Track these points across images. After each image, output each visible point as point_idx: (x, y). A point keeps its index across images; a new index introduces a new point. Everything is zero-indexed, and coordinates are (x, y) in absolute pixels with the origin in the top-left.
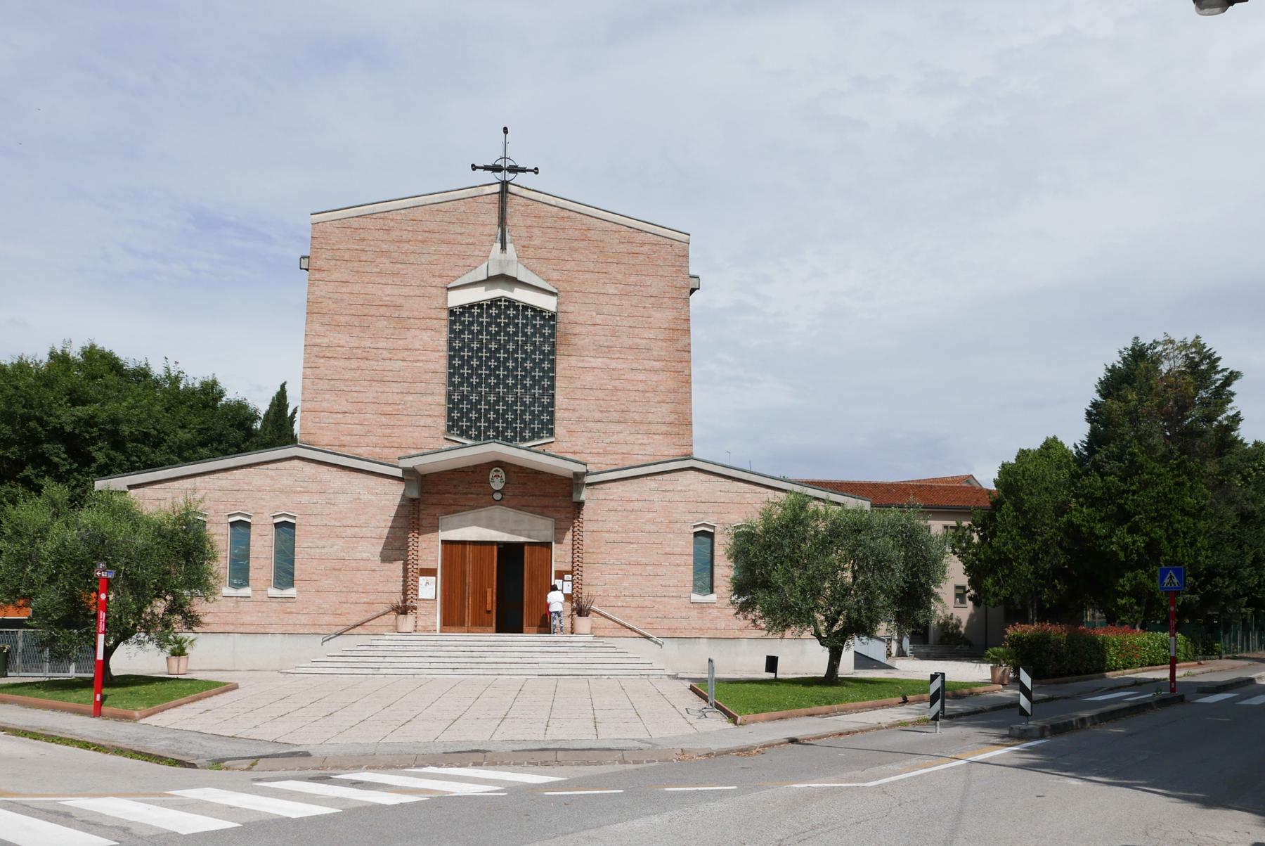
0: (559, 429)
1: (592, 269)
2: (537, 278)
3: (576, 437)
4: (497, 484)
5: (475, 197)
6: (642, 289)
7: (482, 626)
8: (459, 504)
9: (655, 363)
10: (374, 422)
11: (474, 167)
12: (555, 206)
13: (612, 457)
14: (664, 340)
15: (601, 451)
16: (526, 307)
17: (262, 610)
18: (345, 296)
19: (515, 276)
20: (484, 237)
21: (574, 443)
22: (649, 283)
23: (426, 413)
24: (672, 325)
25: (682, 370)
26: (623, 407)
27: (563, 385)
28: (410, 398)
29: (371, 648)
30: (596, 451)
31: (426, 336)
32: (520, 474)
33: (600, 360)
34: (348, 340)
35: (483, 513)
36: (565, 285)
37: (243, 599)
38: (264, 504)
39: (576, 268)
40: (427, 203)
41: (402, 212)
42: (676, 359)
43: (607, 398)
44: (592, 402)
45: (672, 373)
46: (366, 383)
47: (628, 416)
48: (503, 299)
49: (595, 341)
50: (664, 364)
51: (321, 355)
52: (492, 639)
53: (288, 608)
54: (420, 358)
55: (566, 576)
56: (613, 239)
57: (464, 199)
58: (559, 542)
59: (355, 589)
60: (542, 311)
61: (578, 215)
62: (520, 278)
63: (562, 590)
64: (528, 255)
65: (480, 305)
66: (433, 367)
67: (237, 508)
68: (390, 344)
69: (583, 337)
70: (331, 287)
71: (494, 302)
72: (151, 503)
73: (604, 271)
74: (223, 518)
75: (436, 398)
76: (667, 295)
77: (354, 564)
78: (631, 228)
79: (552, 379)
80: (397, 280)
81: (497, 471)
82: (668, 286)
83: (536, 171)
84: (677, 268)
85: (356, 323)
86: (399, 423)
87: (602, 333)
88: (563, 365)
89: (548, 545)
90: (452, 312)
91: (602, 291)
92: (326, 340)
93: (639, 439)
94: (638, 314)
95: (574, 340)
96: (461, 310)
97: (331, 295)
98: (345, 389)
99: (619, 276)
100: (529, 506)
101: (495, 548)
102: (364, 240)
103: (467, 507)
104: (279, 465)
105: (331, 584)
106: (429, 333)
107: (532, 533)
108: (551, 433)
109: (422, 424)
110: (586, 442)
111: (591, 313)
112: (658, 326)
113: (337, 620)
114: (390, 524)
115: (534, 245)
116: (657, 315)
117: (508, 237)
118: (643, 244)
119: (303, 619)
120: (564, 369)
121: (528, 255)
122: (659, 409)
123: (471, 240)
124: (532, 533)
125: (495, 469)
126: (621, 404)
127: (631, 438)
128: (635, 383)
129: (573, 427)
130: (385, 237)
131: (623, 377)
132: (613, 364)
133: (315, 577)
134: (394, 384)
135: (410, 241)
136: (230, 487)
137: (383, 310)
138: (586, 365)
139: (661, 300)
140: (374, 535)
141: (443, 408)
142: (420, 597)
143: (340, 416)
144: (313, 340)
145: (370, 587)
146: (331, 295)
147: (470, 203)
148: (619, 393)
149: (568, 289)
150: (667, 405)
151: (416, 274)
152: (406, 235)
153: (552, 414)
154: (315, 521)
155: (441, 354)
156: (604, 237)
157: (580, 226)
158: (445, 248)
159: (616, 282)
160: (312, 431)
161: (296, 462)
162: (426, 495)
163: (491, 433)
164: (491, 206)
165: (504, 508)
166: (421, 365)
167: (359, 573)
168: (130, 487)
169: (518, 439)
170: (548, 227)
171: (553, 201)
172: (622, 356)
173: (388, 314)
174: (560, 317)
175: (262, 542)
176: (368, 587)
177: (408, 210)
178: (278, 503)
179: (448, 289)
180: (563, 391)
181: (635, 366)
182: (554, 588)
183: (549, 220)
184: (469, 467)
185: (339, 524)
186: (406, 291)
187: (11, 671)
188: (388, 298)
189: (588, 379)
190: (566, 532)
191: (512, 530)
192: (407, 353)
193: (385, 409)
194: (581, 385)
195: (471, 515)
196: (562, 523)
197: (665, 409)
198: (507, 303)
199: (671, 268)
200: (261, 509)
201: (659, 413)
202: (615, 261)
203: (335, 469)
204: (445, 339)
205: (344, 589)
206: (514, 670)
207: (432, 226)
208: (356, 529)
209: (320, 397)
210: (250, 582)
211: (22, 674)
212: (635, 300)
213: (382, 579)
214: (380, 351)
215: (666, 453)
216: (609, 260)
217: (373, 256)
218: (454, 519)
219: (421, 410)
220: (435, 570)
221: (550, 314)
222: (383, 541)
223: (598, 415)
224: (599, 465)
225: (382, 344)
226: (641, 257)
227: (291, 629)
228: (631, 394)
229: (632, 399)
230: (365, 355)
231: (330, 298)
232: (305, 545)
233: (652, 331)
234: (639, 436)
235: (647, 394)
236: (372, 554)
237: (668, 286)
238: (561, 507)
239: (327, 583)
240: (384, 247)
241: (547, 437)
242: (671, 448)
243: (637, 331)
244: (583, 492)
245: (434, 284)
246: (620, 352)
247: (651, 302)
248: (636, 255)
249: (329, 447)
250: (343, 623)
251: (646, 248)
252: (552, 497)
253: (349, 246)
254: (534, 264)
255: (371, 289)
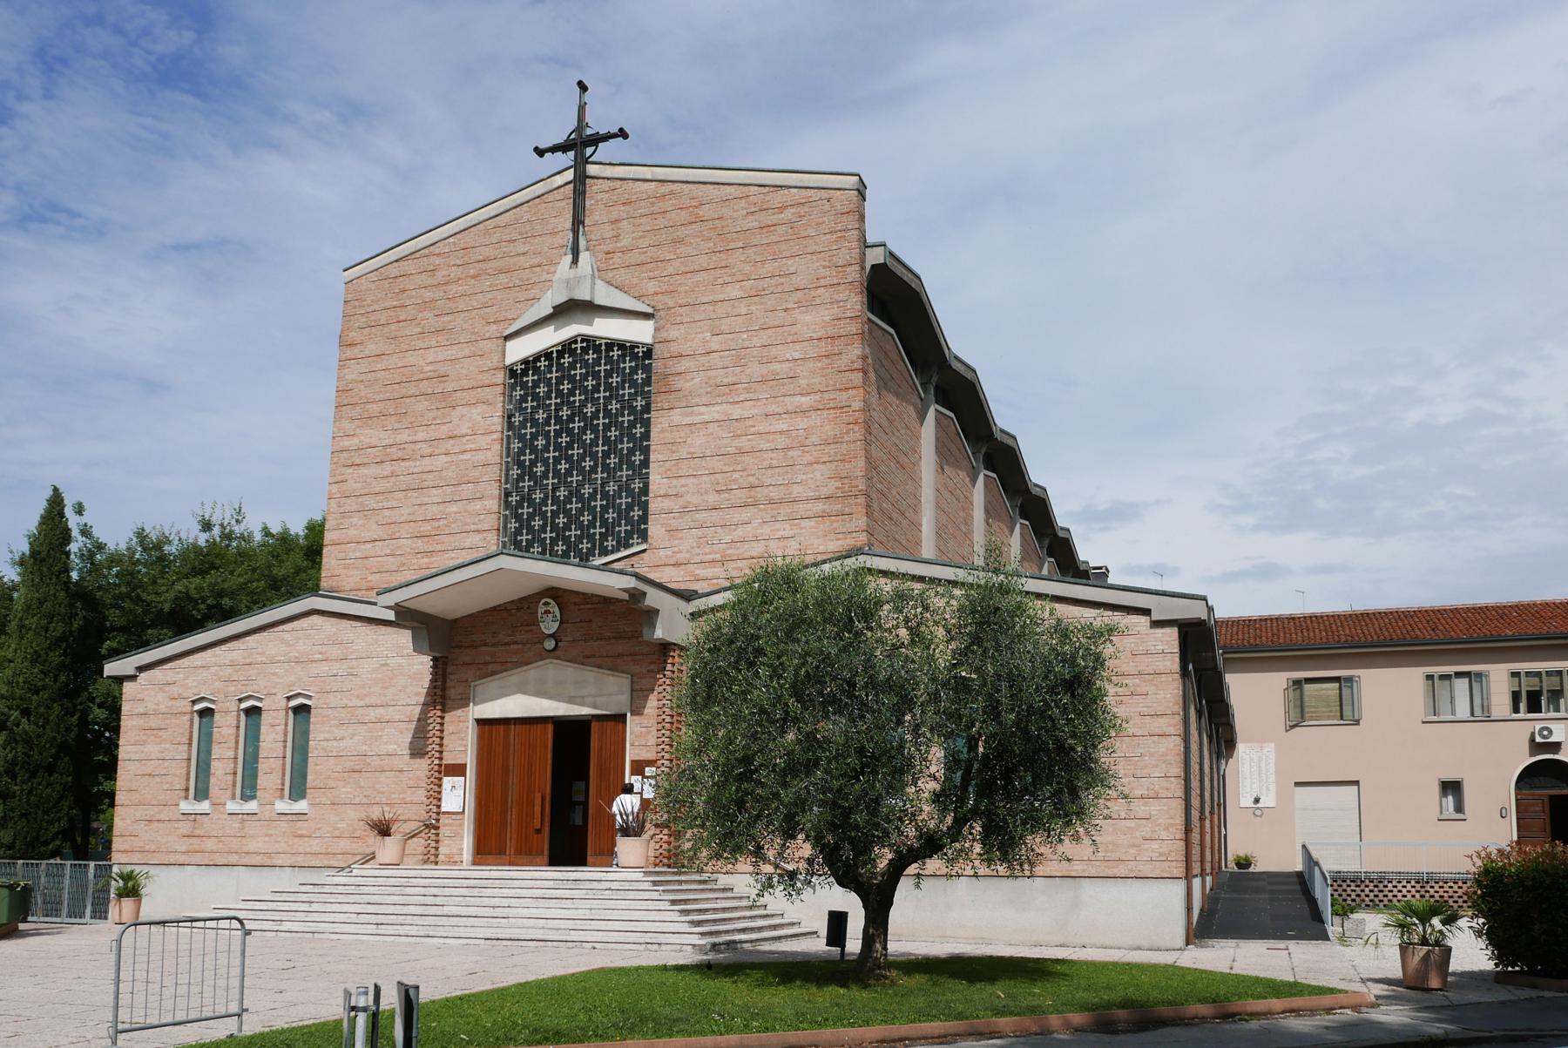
0: (655, 529)
1: (705, 265)
2: (625, 296)
3: (681, 539)
4: (550, 626)
5: (543, 195)
6: (782, 280)
7: (530, 855)
8: (498, 660)
9: (803, 399)
10: (408, 550)
11: (540, 152)
12: (652, 181)
13: (735, 566)
14: (819, 358)
15: (718, 557)
16: (611, 345)
17: (270, 832)
18: (379, 375)
19: (588, 298)
20: (554, 251)
21: (675, 549)
22: (792, 269)
23: (473, 527)
24: (831, 331)
25: (847, 404)
26: (751, 479)
27: (661, 457)
28: (454, 508)
29: (316, 889)
30: (710, 557)
31: (475, 413)
32: (582, 607)
33: (717, 408)
34: (381, 436)
35: (531, 673)
36: (665, 298)
37: (249, 818)
38: (278, 680)
39: (683, 269)
40: (481, 219)
41: (451, 240)
42: (838, 386)
43: (726, 469)
44: (704, 478)
45: (832, 411)
46: (401, 495)
47: (760, 493)
48: (579, 339)
49: (709, 378)
50: (817, 397)
51: (349, 462)
52: (544, 875)
53: (300, 829)
54: (468, 447)
55: (647, 769)
56: (737, 211)
57: (527, 202)
58: (638, 711)
59: (378, 800)
60: (634, 346)
61: (685, 186)
62: (599, 301)
63: (641, 794)
64: (614, 264)
65: (547, 355)
66: (483, 458)
67: (248, 688)
68: (432, 433)
69: (691, 375)
70: (364, 366)
71: (567, 347)
72: (160, 689)
73: (723, 264)
74: (233, 703)
75: (486, 503)
76: (823, 282)
77: (376, 762)
78: (764, 186)
79: (646, 451)
80: (441, 339)
81: (546, 604)
82: (824, 267)
83: (622, 134)
84: (839, 234)
85: (392, 411)
86: (439, 547)
87: (720, 364)
88: (663, 425)
89: (620, 718)
90: (512, 373)
91: (721, 297)
92: (355, 441)
93: (778, 530)
94: (776, 323)
95: (679, 383)
96: (523, 366)
97: (363, 377)
98: (375, 506)
99: (747, 268)
100: (594, 656)
101: (550, 727)
102: (403, 291)
103: (509, 665)
104: (296, 624)
105: (350, 793)
106: (481, 408)
107: (599, 700)
108: (644, 536)
109: (468, 545)
110: (695, 545)
111: (703, 336)
112: (807, 336)
113: (354, 845)
114: (422, 700)
115: (623, 247)
116: (807, 318)
117: (582, 243)
118: (782, 209)
119: (315, 845)
120: (663, 431)
121: (614, 264)
122: (812, 476)
123: (536, 261)
124: (599, 700)
125: (543, 601)
126: (748, 475)
127: (765, 531)
128: (771, 437)
129: (675, 524)
130: (430, 281)
131: (753, 430)
132: (737, 412)
133: (331, 783)
134: (434, 491)
135: (459, 279)
136: (242, 661)
137: (424, 386)
138: (696, 419)
139: (813, 293)
140: (403, 718)
141: (495, 516)
142: (443, 810)
143: (369, 546)
144: (341, 444)
145: (396, 796)
146: (363, 377)
147: (536, 205)
148: (746, 458)
149: (671, 304)
150: (822, 466)
151: (465, 326)
152: (456, 272)
153: (644, 507)
154: (334, 700)
155: (495, 436)
156: (724, 210)
157: (687, 203)
158: (503, 279)
159: (741, 278)
160: (337, 572)
161: (315, 619)
162: (457, 650)
163: (537, 549)
164: (563, 204)
165: (559, 661)
166: (469, 457)
167: (383, 775)
168: (141, 669)
169: (597, 552)
170: (642, 216)
171: (646, 173)
172: (752, 396)
173: (430, 391)
174: (657, 353)
175: (274, 736)
176: (393, 796)
177: (458, 236)
178: (292, 678)
179: (507, 338)
180: (661, 466)
181: (772, 408)
182: (629, 789)
183: (643, 203)
184: (513, 601)
185: (361, 703)
186: (451, 352)
187: (33, 915)
188: (430, 368)
189: (698, 442)
190: (648, 696)
191: (571, 697)
192: (452, 442)
193: (422, 529)
194: (688, 453)
195: (515, 677)
196: (643, 681)
197: (820, 472)
198: (585, 344)
199: (828, 236)
200: (274, 688)
201: (810, 481)
202: (741, 245)
203: (359, 624)
204: (501, 414)
205: (365, 800)
206: (461, 929)
207: (487, 252)
208: (381, 710)
209: (346, 523)
210: (258, 793)
211: (42, 919)
212: (770, 302)
213: (411, 783)
214: (419, 445)
215: (822, 549)
216: (732, 245)
217: (413, 312)
218: (492, 684)
219: (466, 524)
220: (464, 766)
221: (645, 349)
222: (413, 725)
223: (712, 499)
224: (715, 581)
225: (421, 435)
226: (780, 229)
227: (300, 860)
228: (765, 456)
229: (766, 464)
230: (400, 454)
231: (362, 381)
232: (321, 736)
233: (797, 346)
234: (778, 525)
235: (791, 453)
236: (399, 746)
237: (824, 267)
238: (642, 654)
239: (344, 792)
240: (428, 295)
241: (638, 544)
242: (830, 540)
243: (774, 351)
244: (658, 625)
245: (487, 335)
246: (747, 390)
247: (796, 299)
248: (772, 228)
249: (355, 593)
250: (360, 851)
251: (788, 214)
252: (629, 638)
253: (387, 304)
254: (622, 276)
255: (411, 359)
